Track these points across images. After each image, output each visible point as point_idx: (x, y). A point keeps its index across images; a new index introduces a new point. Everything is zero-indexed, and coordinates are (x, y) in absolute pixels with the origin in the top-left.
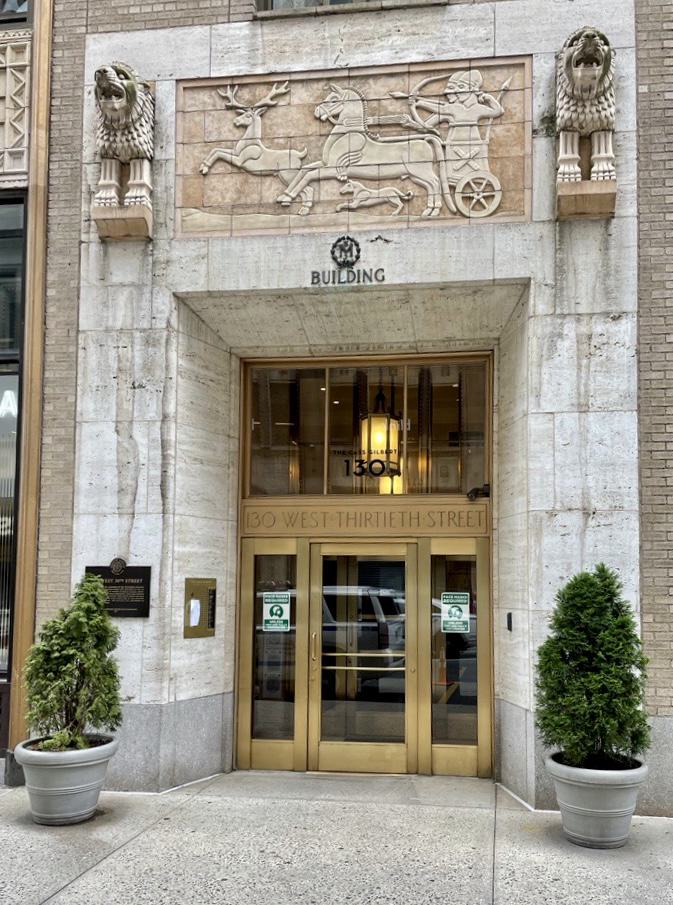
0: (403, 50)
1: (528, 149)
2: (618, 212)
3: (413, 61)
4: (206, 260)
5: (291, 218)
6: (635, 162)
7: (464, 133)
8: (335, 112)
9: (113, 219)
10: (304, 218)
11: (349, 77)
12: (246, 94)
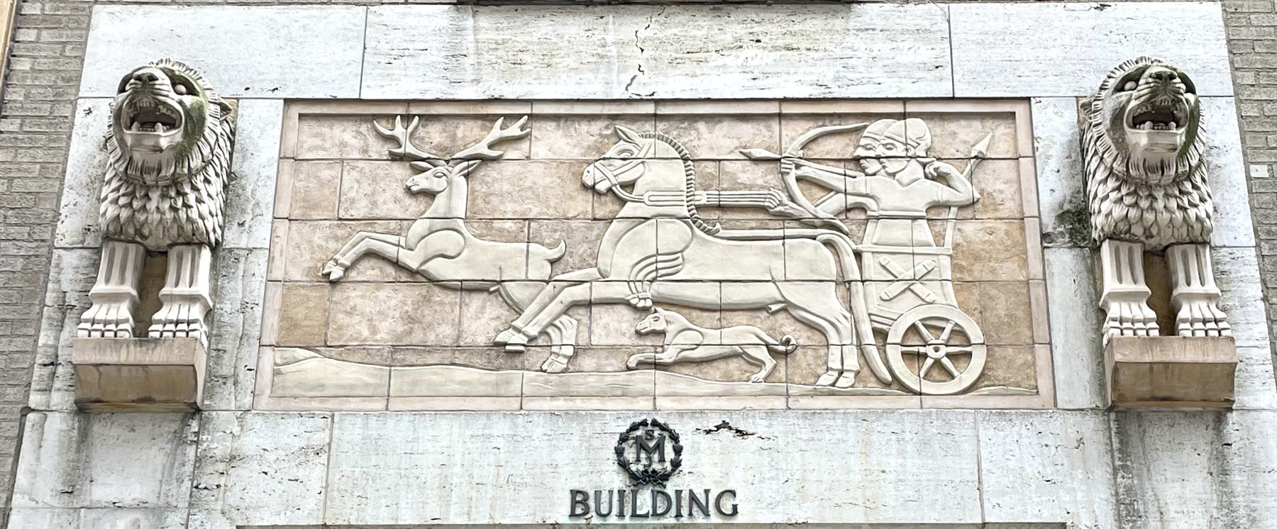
0: (767, 75)
1: (1035, 268)
2: (1240, 399)
3: (790, 95)
4: (324, 457)
5: (519, 379)
6: (1261, 305)
7: (899, 232)
9: (119, 366)
10: (553, 377)
11: (656, 117)
12: (435, 134)
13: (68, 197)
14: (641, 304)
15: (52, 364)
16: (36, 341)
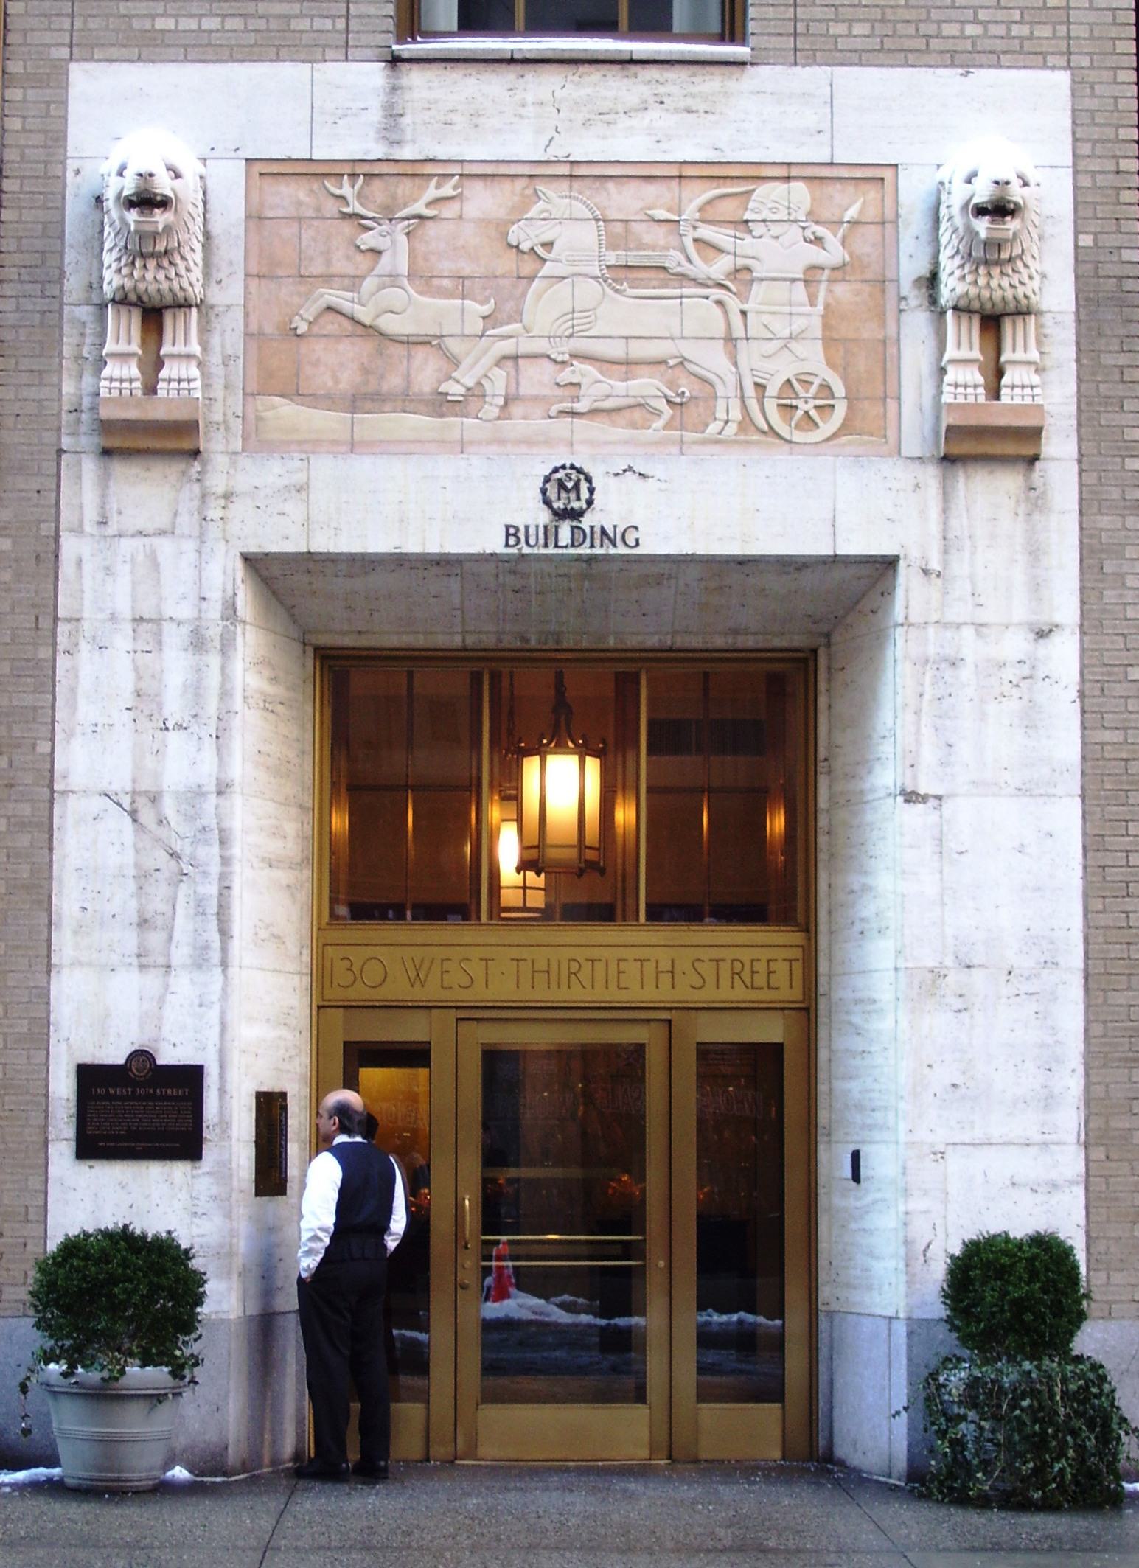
1: (891, 330)
4: (304, 494)
8: (546, 238)
13: (70, 256)
14: (560, 359)
15: (76, 410)
16: (60, 390)
